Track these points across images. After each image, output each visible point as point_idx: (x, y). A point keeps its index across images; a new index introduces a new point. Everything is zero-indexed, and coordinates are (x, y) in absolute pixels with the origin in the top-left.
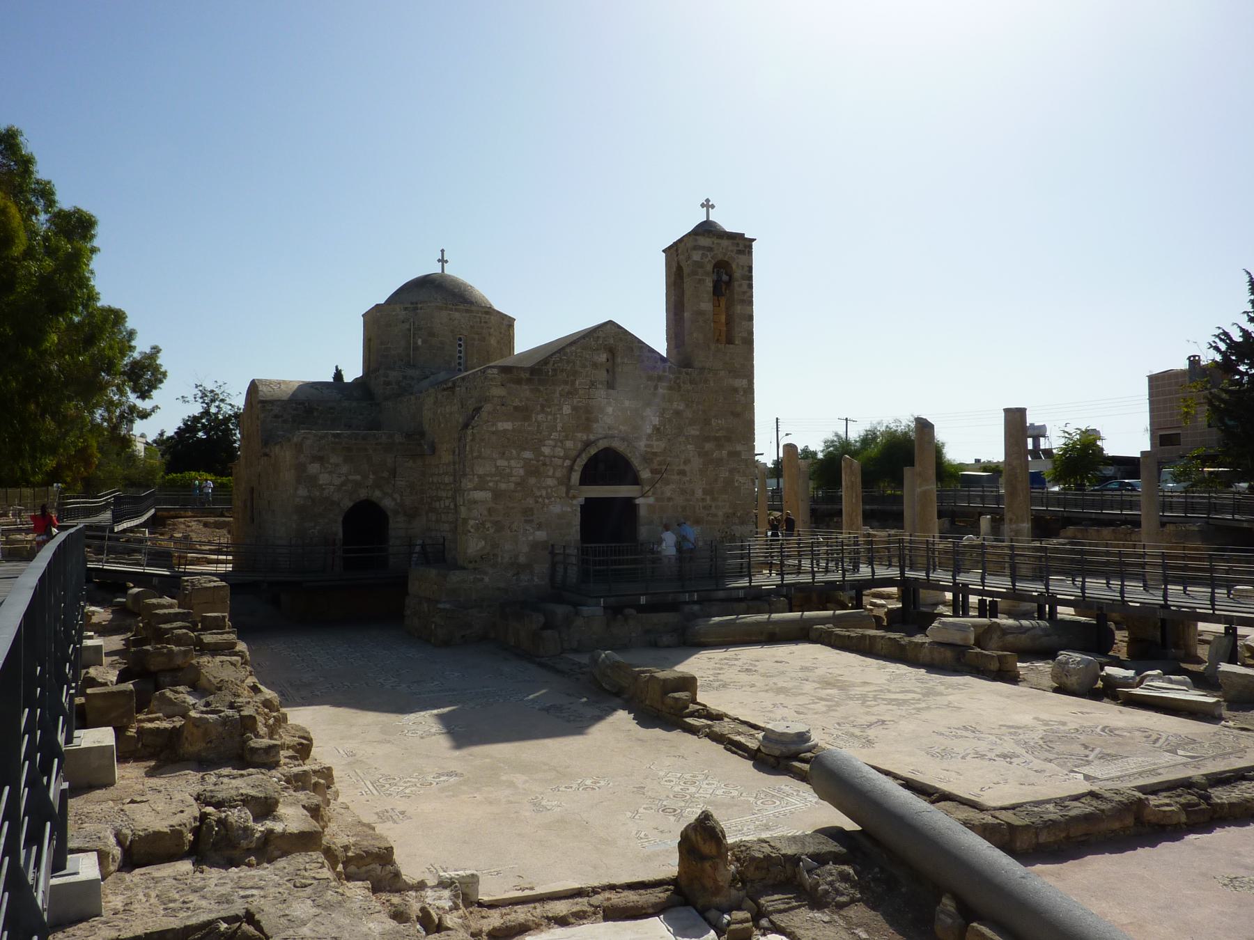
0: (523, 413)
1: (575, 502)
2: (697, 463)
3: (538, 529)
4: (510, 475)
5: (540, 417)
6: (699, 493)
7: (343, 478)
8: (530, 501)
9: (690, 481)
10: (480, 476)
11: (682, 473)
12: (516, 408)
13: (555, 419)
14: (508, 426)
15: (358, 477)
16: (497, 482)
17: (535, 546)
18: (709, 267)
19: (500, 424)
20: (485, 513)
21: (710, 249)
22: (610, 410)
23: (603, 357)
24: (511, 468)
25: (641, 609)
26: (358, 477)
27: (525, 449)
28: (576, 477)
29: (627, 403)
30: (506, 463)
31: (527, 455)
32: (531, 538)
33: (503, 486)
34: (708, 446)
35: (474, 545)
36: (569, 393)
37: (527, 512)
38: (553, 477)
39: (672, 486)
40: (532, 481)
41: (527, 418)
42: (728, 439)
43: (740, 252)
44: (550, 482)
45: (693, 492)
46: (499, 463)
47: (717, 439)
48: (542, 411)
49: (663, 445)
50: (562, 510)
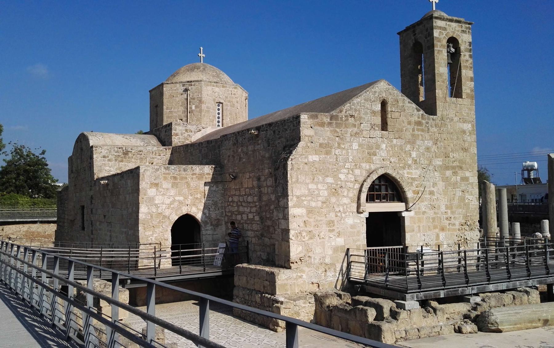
1: (362, 215)
2: (441, 185)
3: (338, 236)
4: (318, 195)
5: (338, 152)
6: (443, 208)
7: (171, 200)
8: (332, 215)
9: (437, 199)
10: (298, 197)
11: (431, 193)
12: (321, 145)
13: (348, 153)
14: (316, 158)
15: (181, 198)
16: (309, 201)
17: (336, 249)
18: (445, 42)
19: (310, 157)
20: (302, 225)
21: (445, 29)
22: (384, 146)
23: (378, 107)
24: (317, 189)
25: (441, 301)
26: (181, 198)
27: (327, 176)
28: (364, 196)
29: (395, 141)
30: (315, 187)
31: (330, 180)
32: (333, 244)
33: (313, 204)
34: (448, 173)
35: (295, 250)
36: (356, 133)
37: (330, 223)
38: (347, 196)
39: (426, 203)
40: (333, 200)
41: (327, 153)
42: (461, 168)
43: (463, 31)
44: (346, 201)
45: (439, 206)
46: (311, 186)
47: (453, 168)
48: (339, 147)
49: (419, 173)
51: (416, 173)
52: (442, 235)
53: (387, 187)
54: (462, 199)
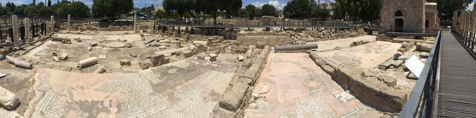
0: (388, 5)
11: (410, 14)
28: (394, 15)
50: (392, 20)
51: (406, 9)
52: (412, 24)
53: (399, 13)
54: (418, 15)
